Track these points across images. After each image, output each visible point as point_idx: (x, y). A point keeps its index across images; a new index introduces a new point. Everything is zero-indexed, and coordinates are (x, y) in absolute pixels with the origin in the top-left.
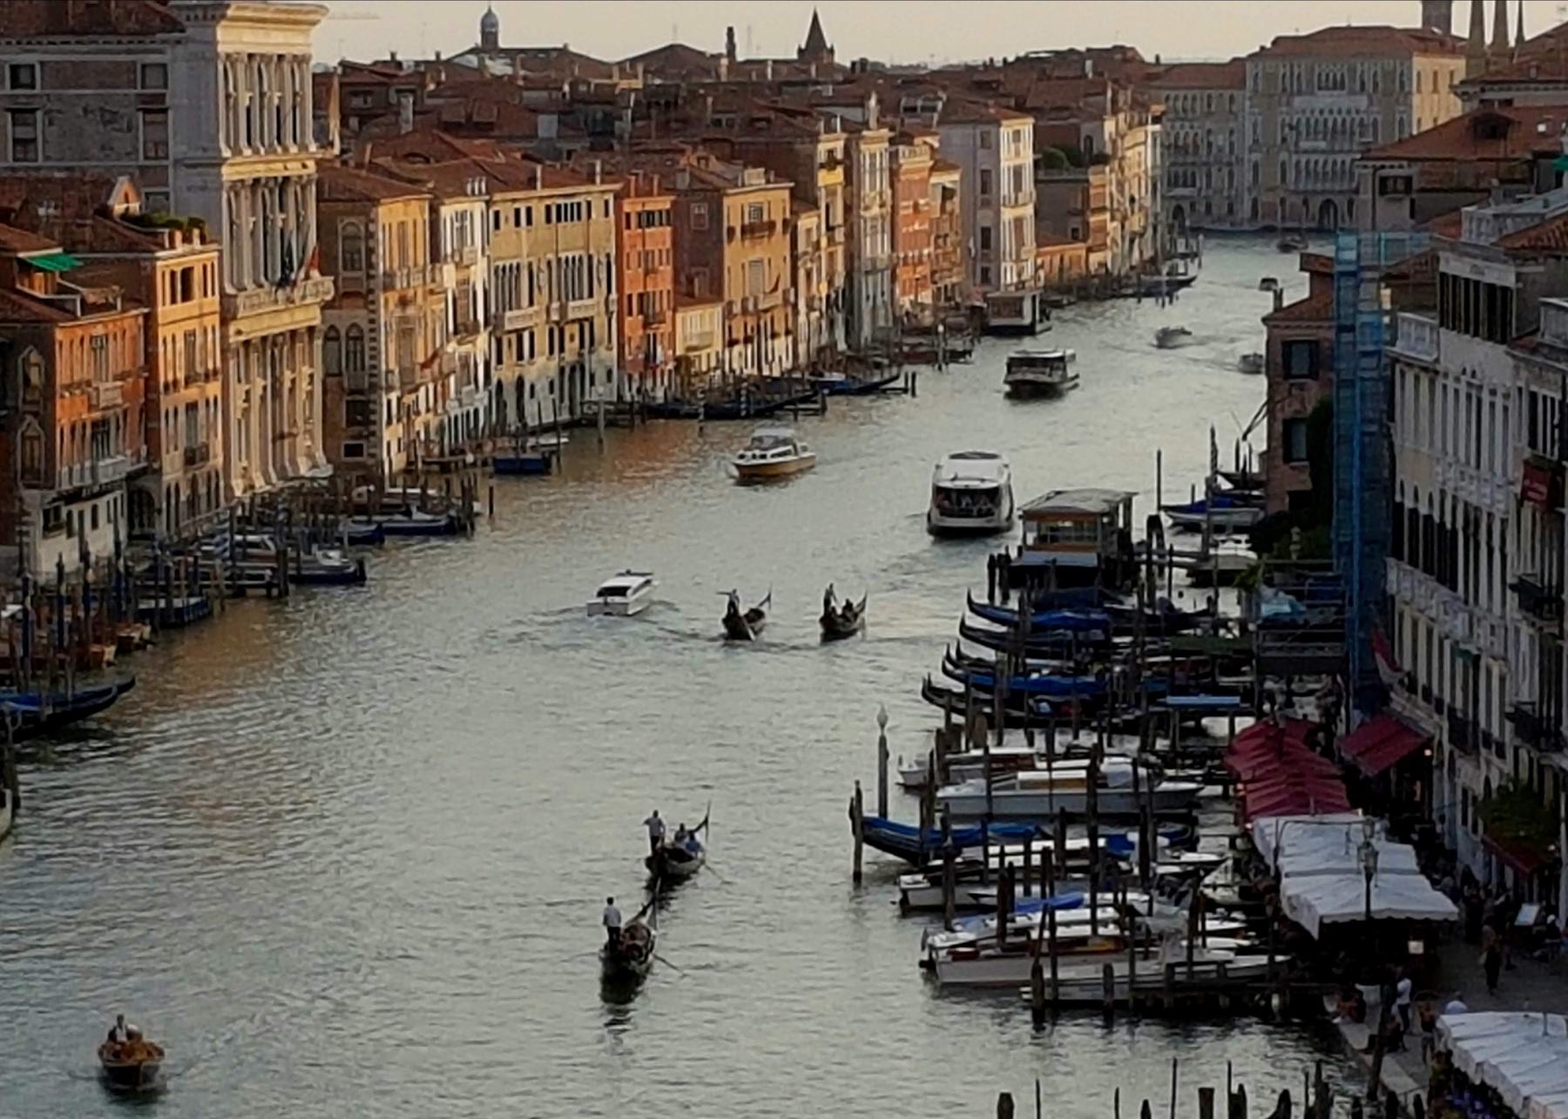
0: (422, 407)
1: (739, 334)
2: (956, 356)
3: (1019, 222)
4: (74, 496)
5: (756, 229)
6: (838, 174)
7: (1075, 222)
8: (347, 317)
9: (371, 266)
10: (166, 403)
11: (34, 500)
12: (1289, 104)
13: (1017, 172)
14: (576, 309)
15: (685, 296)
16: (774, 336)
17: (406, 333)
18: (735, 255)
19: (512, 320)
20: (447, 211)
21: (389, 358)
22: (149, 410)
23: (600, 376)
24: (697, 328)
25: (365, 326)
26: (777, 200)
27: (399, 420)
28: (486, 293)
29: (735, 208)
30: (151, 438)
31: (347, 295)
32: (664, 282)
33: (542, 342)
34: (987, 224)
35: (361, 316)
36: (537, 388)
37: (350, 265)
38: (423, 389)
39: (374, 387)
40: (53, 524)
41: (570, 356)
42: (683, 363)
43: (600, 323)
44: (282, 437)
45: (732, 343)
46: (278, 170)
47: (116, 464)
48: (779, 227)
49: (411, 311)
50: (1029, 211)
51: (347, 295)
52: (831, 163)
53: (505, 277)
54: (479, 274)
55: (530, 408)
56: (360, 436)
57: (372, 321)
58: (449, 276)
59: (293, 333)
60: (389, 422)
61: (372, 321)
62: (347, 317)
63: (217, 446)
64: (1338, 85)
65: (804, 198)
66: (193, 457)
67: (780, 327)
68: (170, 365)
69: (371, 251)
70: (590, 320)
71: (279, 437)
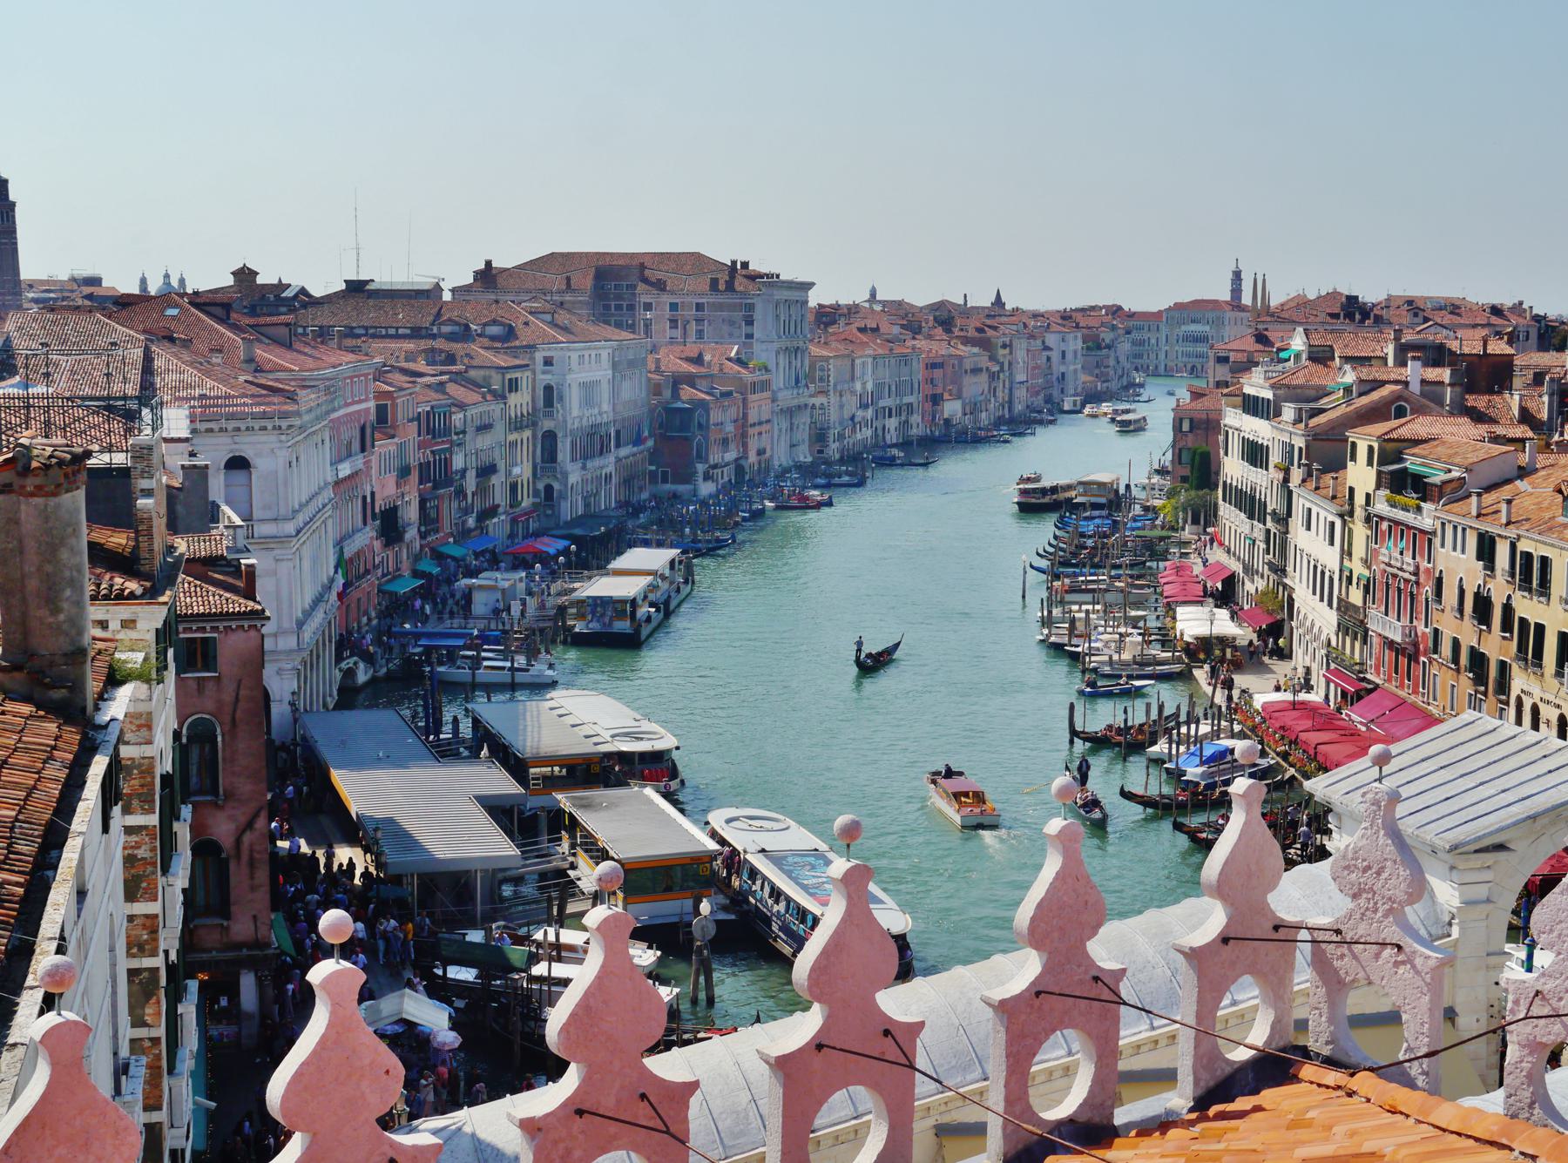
2: (1051, 422)
4: (715, 467)
5: (976, 371)
8: (818, 401)
10: (751, 431)
11: (700, 468)
13: (1075, 352)
14: (907, 400)
17: (842, 407)
18: (968, 380)
19: (882, 403)
20: (858, 362)
21: (834, 416)
22: (744, 435)
26: (984, 362)
30: (745, 445)
37: (821, 380)
40: (707, 477)
42: (947, 421)
46: (795, 344)
47: (731, 456)
52: (1004, 346)
53: (879, 386)
54: (870, 387)
55: (888, 437)
58: (858, 386)
62: (818, 401)
66: (760, 452)
68: (752, 418)
71: (792, 446)
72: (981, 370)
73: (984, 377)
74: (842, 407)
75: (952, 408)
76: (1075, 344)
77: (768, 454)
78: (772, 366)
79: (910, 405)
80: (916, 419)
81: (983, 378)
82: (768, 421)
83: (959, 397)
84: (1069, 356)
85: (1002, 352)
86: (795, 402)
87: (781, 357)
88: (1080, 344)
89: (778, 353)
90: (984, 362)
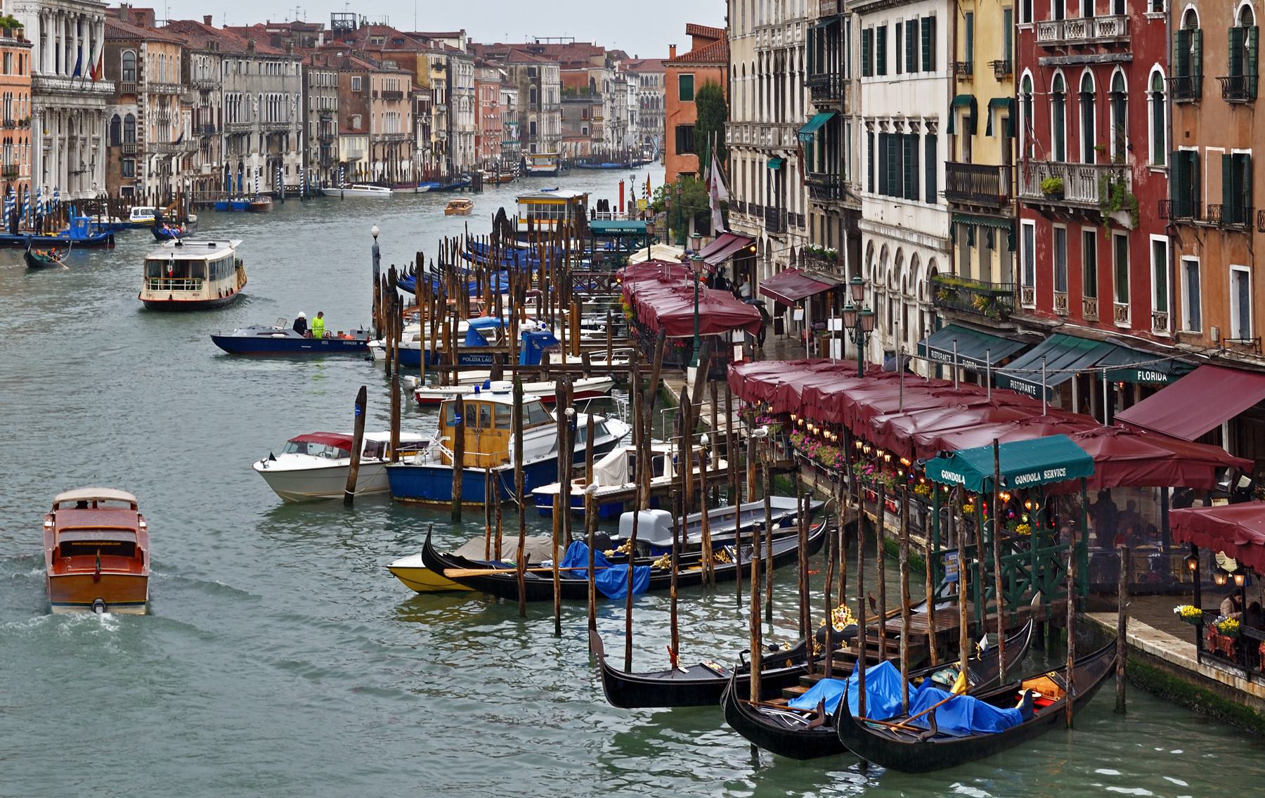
0: (174, 170)
1: (379, 155)
5: (392, 97)
6: (443, 75)
7: (585, 125)
8: (125, 109)
9: (141, 78)
16: (402, 159)
17: (164, 123)
18: (377, 107)
23: (292, 169)
25: (136, 115)
26: (403, 83)
27: (157, 175)
28: (220, 110)
33: (255, 140)
35: (133, 109)
36: (252, 171)
38: (174, 160)
44: (76, 173)
45: (375, 160)
48: (405, 96)
49: (168, 110)
52: (438, 67)
59: (86, 111)
60: (150, 175)
63: (24, 170)
69: (140, 69)
71: (71, 173)
72: (400, 94)
73: (405, 107)
74: (164, 123)
77: (24, 178)
78: (32, 33)
80: (293, 159)
82: (25, 123)
83: (365, 131)
86: (79, 103)
87: (50, 26)
89: (43, 18)
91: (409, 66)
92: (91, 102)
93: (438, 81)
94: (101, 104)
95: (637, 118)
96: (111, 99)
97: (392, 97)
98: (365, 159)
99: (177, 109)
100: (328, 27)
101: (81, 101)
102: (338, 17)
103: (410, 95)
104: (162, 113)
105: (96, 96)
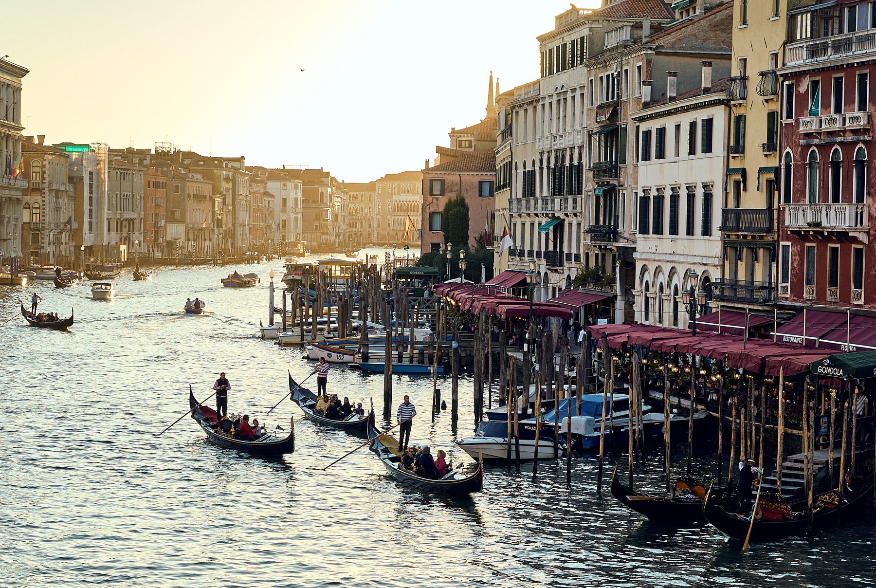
1: (191, 237)
3: (296, 220)
5: (199, 198)
6: (230, 185)
7: (317, 223)
9: (44, 178)
12: (391, 198)
13: (296, 200)
14: (127, 215)
15: (171, 219)
16: (205, 240)
17: (58, 209)
18: (190, 205)
24: (175, 231)
29: (191, 188)
31: (33, 190)
32: (162, 212)
34: (284, 218)
35: (39, 198)
39: (44, 228)
41: (124, 235)
42: (170, 244)
43: (137, 222)
45: (189, 240)
49: (60, 201)
50: (300, 216)
51: (33, 190)
52: (227, 179)
56: (37, 249)
57: (44, 201)
61: (44, 201)
64: (409, 192)
65: (216, 191)
67: (207, 237)
69: (44, 173)
70: (133, 220)
72: (205, 197)
74: (58, 209)
75: (175, 231)
76: (295, 193)
79: (131, 221)
81: (207, 204)
83: (182, 221)
84: (290, 204)
85: (225, 185)
88: (299, 195)
90: (207, 189)
91: (209, 177)
92: (13, 192)
93: (227, 189)
94: (18, 194)
95: (347, 222)
96: (25, 192)
97: (199, 198)
98: (183, 239)
99: (66, 200)
100: (153, 152)
101: (7, 192)
102: (159, 145)
103: (211, 197)
104: (57, 203)
105: (16, 189)
